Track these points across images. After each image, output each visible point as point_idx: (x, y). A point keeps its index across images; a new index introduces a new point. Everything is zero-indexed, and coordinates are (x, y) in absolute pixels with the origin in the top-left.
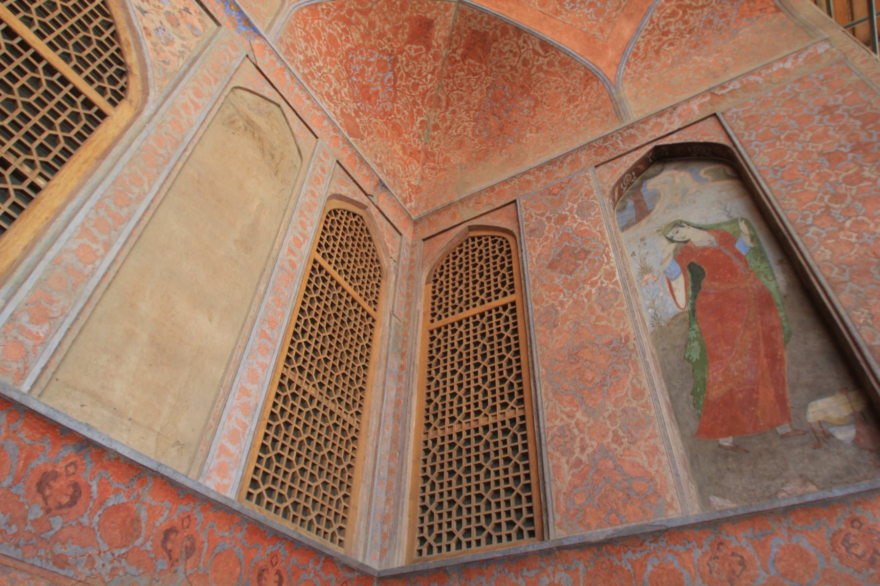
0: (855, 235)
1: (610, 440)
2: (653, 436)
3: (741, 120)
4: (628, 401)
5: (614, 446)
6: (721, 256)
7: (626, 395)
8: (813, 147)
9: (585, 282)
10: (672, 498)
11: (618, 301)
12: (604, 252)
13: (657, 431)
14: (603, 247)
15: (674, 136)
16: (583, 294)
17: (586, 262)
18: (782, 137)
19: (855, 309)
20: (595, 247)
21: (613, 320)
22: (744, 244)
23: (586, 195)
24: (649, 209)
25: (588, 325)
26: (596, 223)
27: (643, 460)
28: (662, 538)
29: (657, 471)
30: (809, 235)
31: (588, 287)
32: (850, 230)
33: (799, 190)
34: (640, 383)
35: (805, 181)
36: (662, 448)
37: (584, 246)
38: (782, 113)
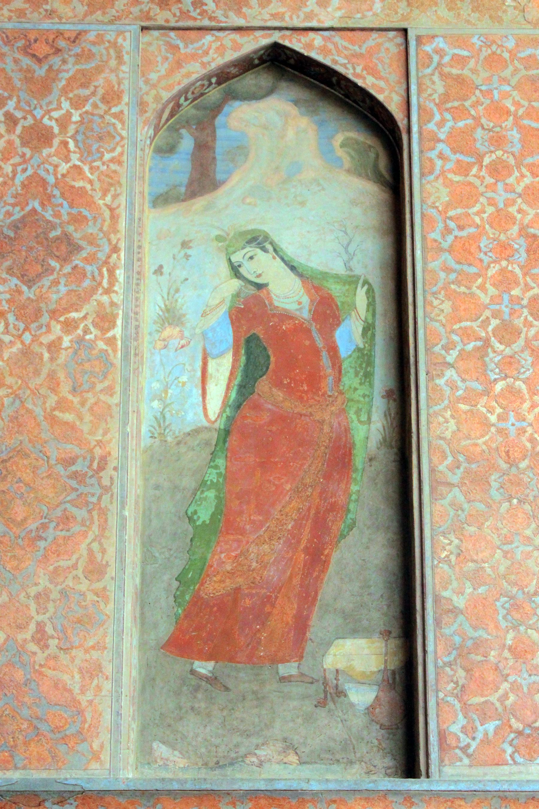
0: (499, 410)
1: (28, 635)
2: (99, 647)
3: (444, 76)
4: (76, 577)
5: (32, 647)
6: (307, 343)
7: (75, 566)
8: (519, 211)
9: (54, 314)
10: (102, 746)
11: (106, 383)
12: (106, 262)
13: (108, 639)
14: (107, 249)
15: (317, 39)
16: (46, 340)
17: (68, 269)
18: (487, 160)
19: (444, 534)
20: (92, 241)
21: (88, 418)
22: (349, 336)
23: (104, 99)
24: (219, 176)
25: (38, 411)
26: (110, 183)
27: (73, 681)
28: (71, 801)
29: (90, 702)
30: (441, 382)
31: (57, 329)
32: (496, 398)
33: (463, 289)
34: (103, 551)
35: (478, 275)
36: (108, 669)
37: (71, 229)
38: (508, 103)
